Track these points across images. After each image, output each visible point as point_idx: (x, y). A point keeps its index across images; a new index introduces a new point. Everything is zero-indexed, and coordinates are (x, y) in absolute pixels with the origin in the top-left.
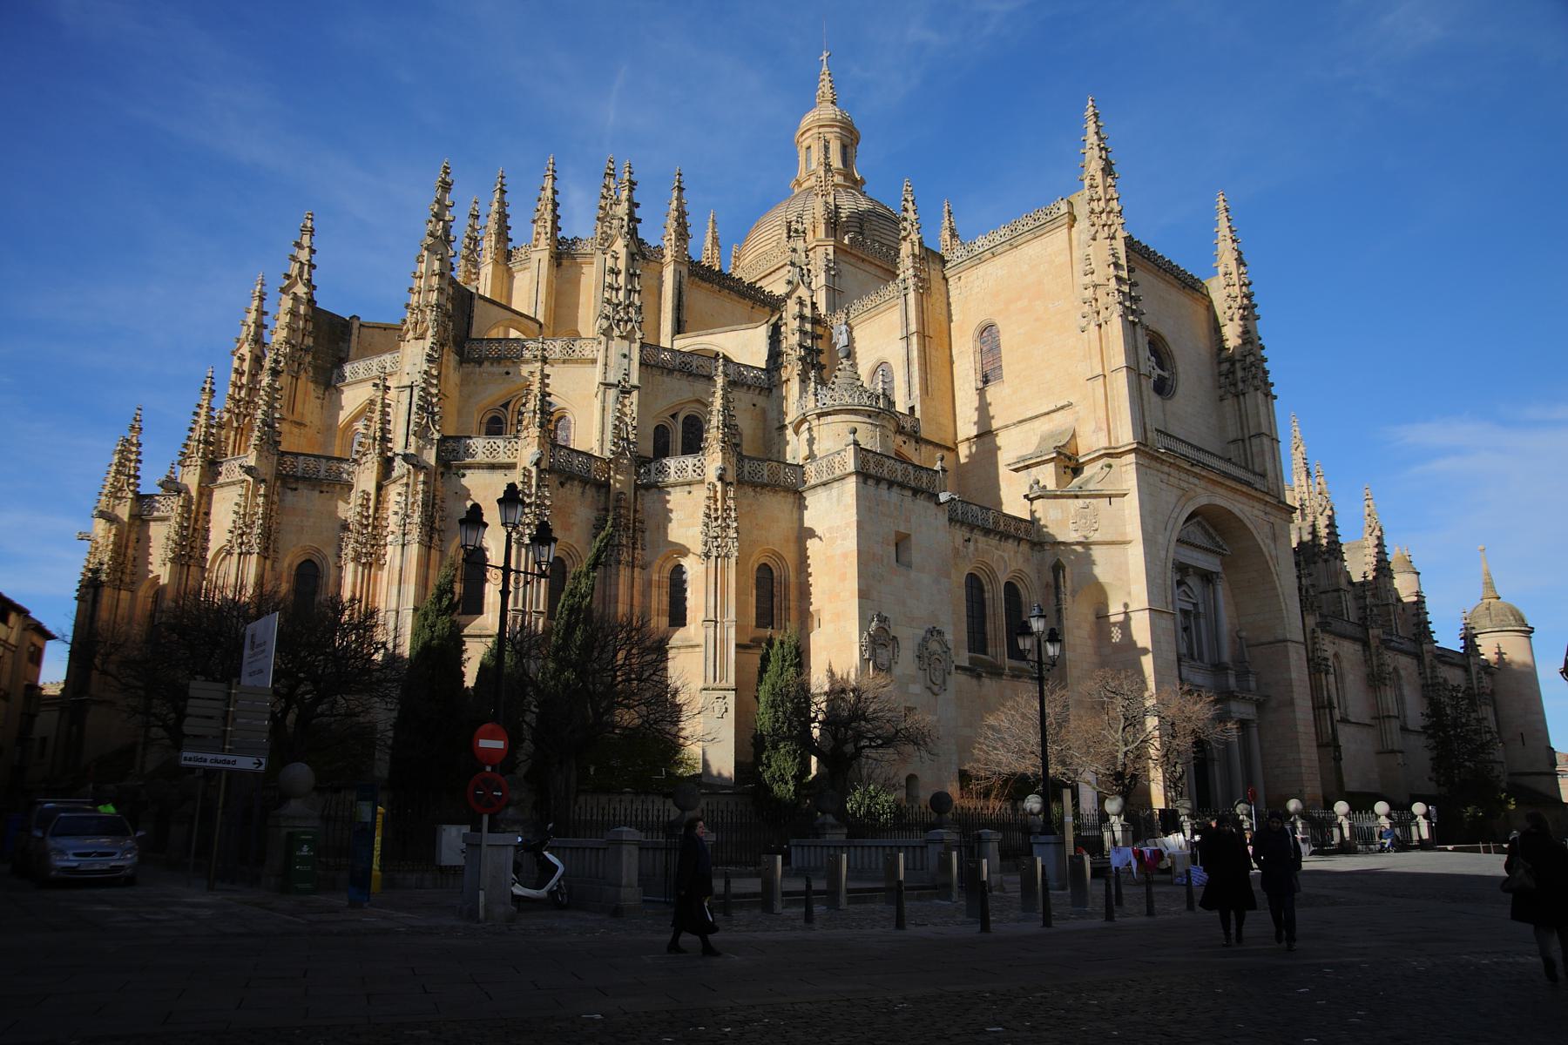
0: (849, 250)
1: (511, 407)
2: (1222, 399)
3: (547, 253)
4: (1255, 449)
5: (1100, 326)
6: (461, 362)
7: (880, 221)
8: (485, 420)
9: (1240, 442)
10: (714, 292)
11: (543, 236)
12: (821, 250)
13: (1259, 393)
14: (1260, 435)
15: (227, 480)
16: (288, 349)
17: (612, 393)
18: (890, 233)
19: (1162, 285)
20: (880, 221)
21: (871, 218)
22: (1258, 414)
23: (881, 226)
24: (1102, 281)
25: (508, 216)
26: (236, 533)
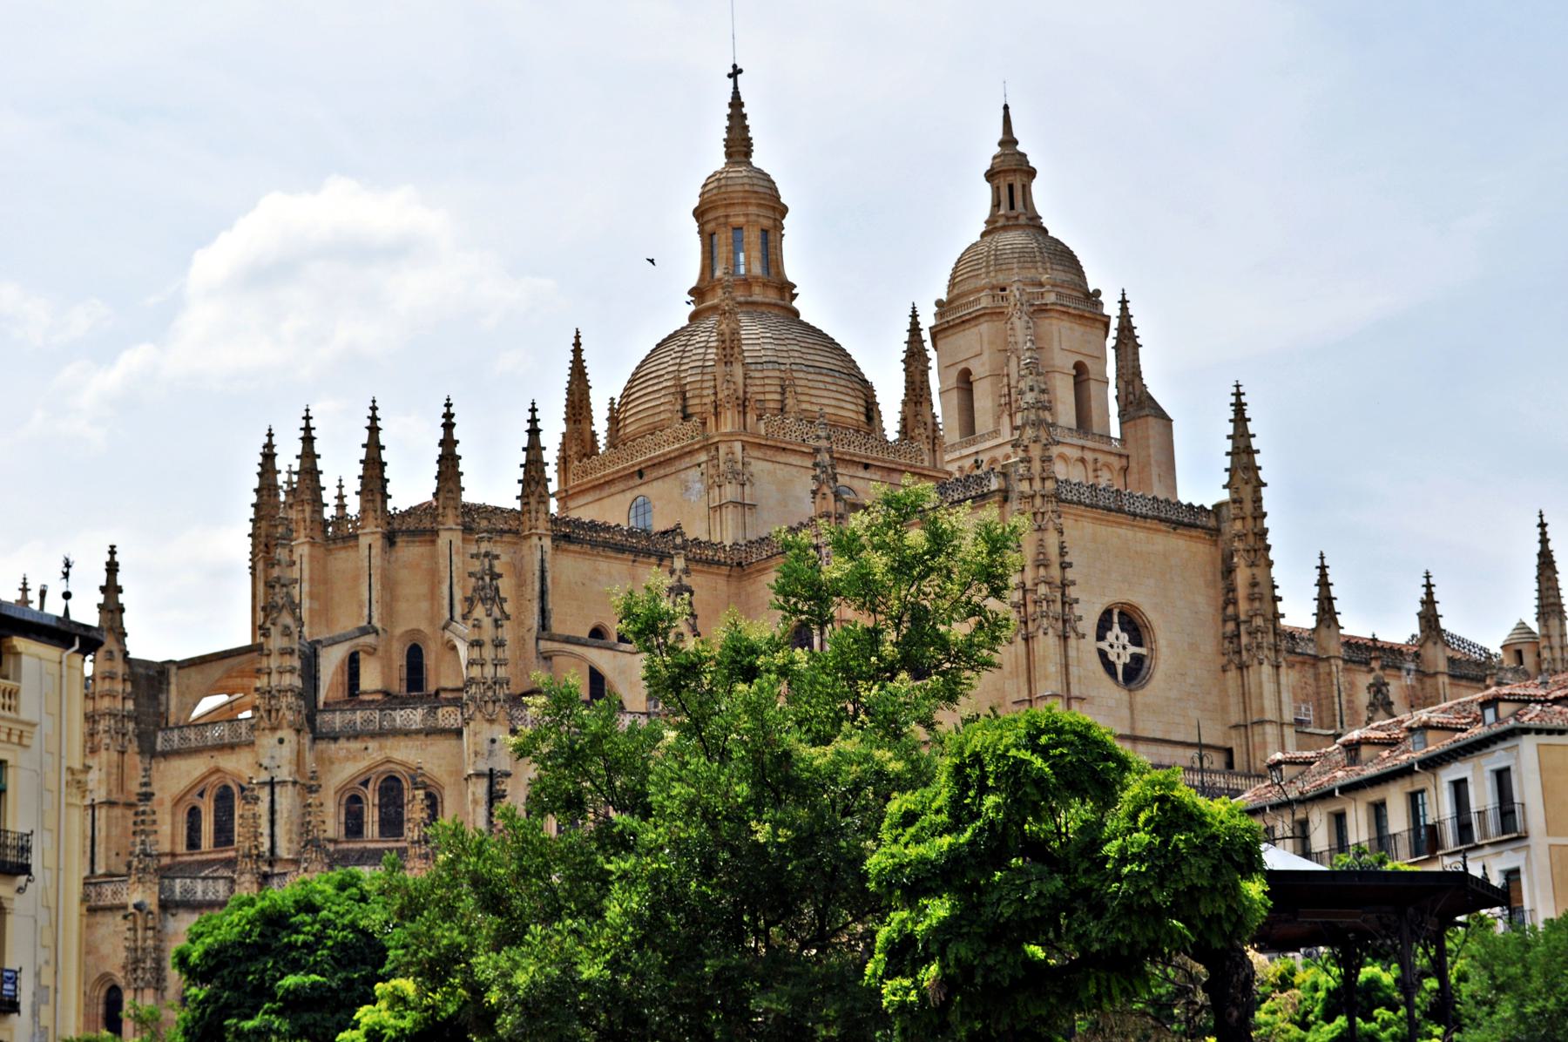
0: (763, 442)
1: (371, 786)
2: (1224, 670)
3: (378, 536)
4: (1257, 739)
5: (1026, 639)
6: (314, 740)
7: (810, 377)
8: (344, 801)
9: (1243, 729)
10: (585, 553)
11: (372, 514)
12: (723, 449)
13: (1267, 669)
14: (1262, 722)
15: (101, 903)
16: (112, 722)
17: (484, 783)
18: (825, 393)
19: (1141, 535)
20: (810, 377)
21: (795, 374)
22: (1261, 695)
23: (810, 384)
24: (1029, 585)
25: (321, 472)
26: (130, 967)
